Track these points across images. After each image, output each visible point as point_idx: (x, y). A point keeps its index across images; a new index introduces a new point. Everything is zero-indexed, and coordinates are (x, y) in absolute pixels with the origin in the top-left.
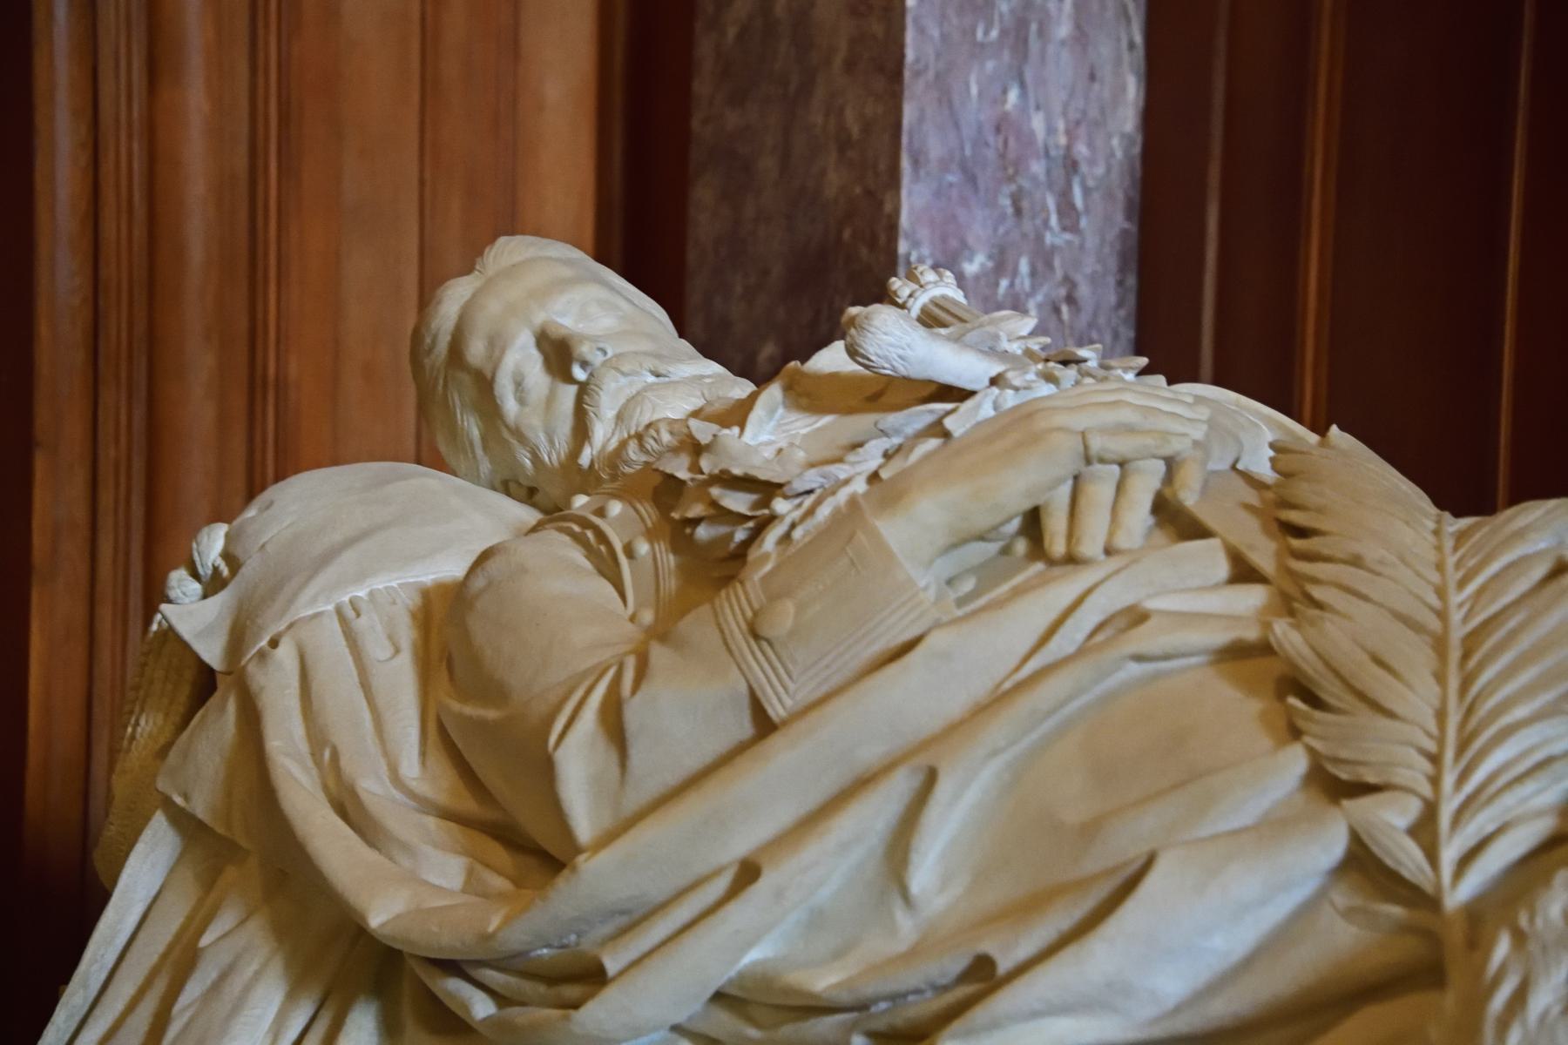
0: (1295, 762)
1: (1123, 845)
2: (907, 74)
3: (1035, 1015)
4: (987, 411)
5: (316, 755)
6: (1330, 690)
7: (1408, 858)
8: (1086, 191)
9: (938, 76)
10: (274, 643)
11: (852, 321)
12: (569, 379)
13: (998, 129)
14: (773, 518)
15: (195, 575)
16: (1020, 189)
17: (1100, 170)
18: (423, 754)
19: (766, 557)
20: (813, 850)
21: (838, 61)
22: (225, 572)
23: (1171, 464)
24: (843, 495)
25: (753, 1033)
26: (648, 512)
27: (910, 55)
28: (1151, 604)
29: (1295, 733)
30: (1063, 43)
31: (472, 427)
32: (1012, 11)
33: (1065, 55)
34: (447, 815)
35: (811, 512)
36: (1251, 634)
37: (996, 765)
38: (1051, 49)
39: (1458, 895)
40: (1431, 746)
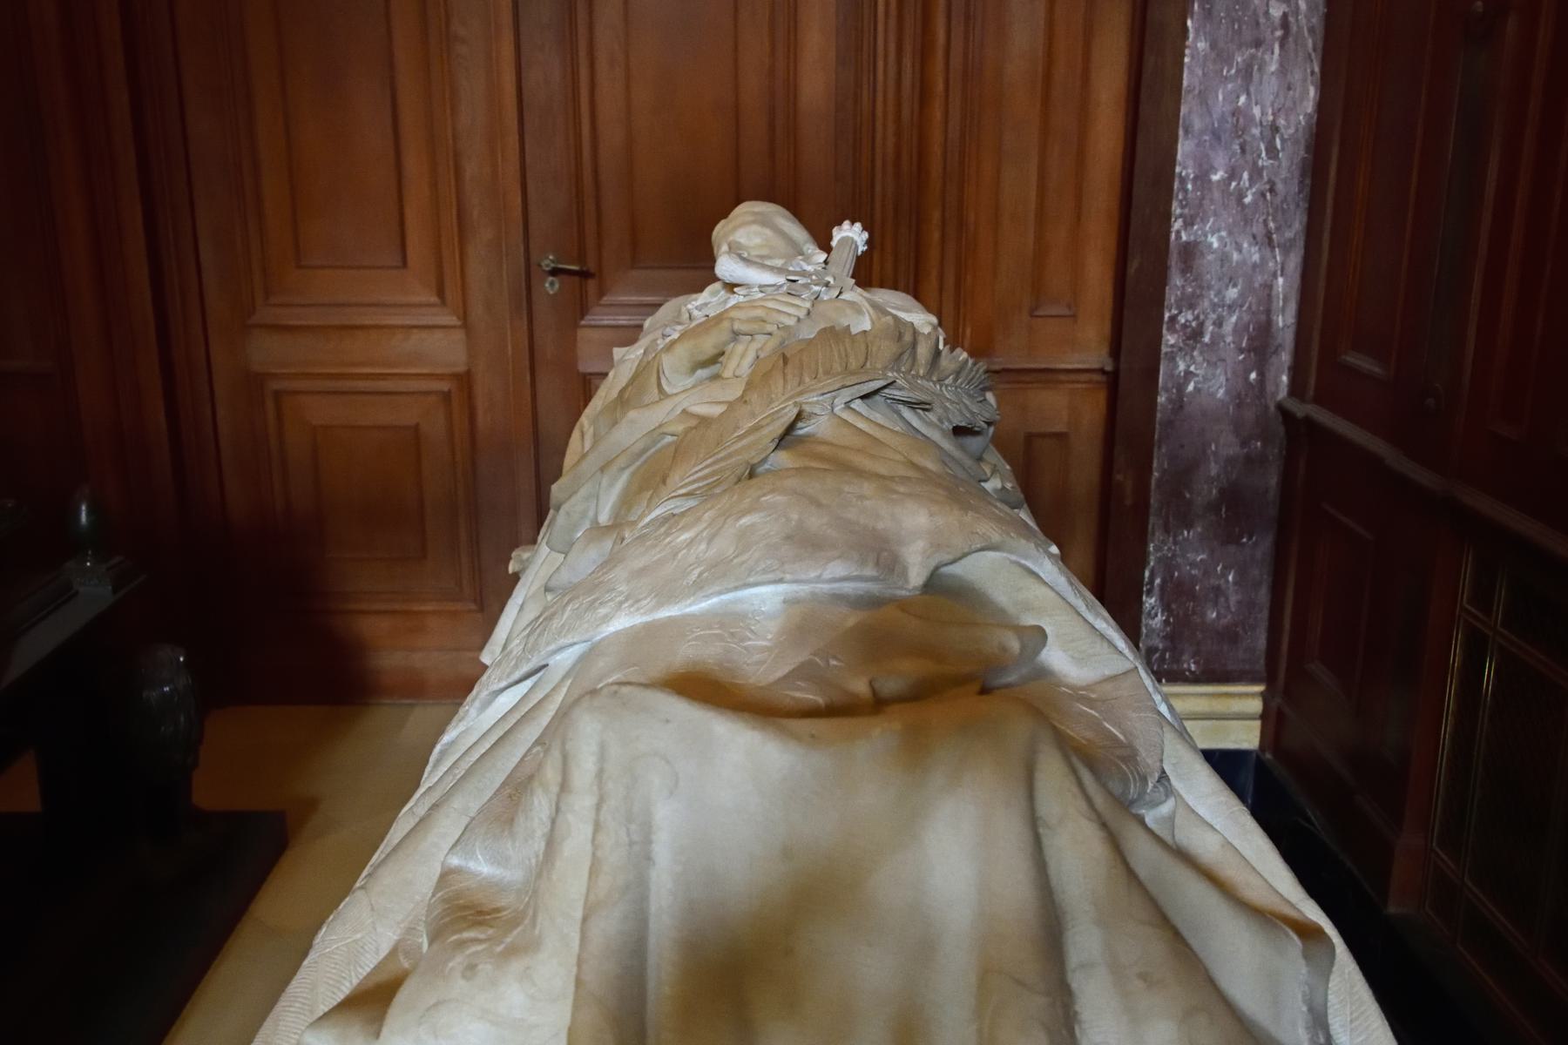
8: (1283, 141)
9: (1200, 92)
13: (1233, 115)
16: (1245, 141)
17: (1291, 131)
27: (1185, 83)
30: (1273, 73)
32: (1244, 61)
33: (1274, 79)
37: (625, 477)
38: (1265, 77)
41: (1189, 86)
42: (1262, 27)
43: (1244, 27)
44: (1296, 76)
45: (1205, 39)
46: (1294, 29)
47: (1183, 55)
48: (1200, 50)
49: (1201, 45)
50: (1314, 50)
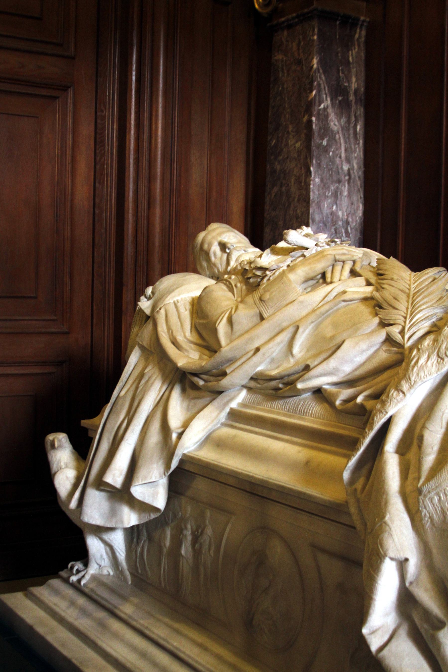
0: (376, 320)
1: (338, 340)
2: (311, 202)
3: (318, 376)
4: (314, 251)
5: (168, 332)
6: (385, 305)
7: (398, 338)
8: (351, 229)
9: (317, 202)
10: (160, 309)
11: (285, 233)
12: (225, 252)
13: (331, 214)
14: (266, 275)
15: (146, 297)
16: (336, 228)
17: (354, 224)
18: (191, 332)
19: (264, 283)
20: (271, 344)
21: (296, 200)
22: (152, 296)
23: (354, 262)
24: (281, 270)
25: (259, 386)
26: (240, 278)
27: (311, 198)
28: (347, 290)
29: (377, 315)
30: (345, 196)
31: (205, 264)
32: (334, 189)
33: (346, 199)
34: (196, 344)
35: (274, 273)
36: (369, 295)
37: (312, 325)
38: (343, 197)
39: (408, 345)
40: (405, 315)
41: (313, 199)
42: (340, 174)
43: (333, 173)
44: (355, 198)
45: (319, 177)
46: (353, 176)
47: (310, 185)
48: (317, 182)
49: (317, 180)
50: (361, 187)
